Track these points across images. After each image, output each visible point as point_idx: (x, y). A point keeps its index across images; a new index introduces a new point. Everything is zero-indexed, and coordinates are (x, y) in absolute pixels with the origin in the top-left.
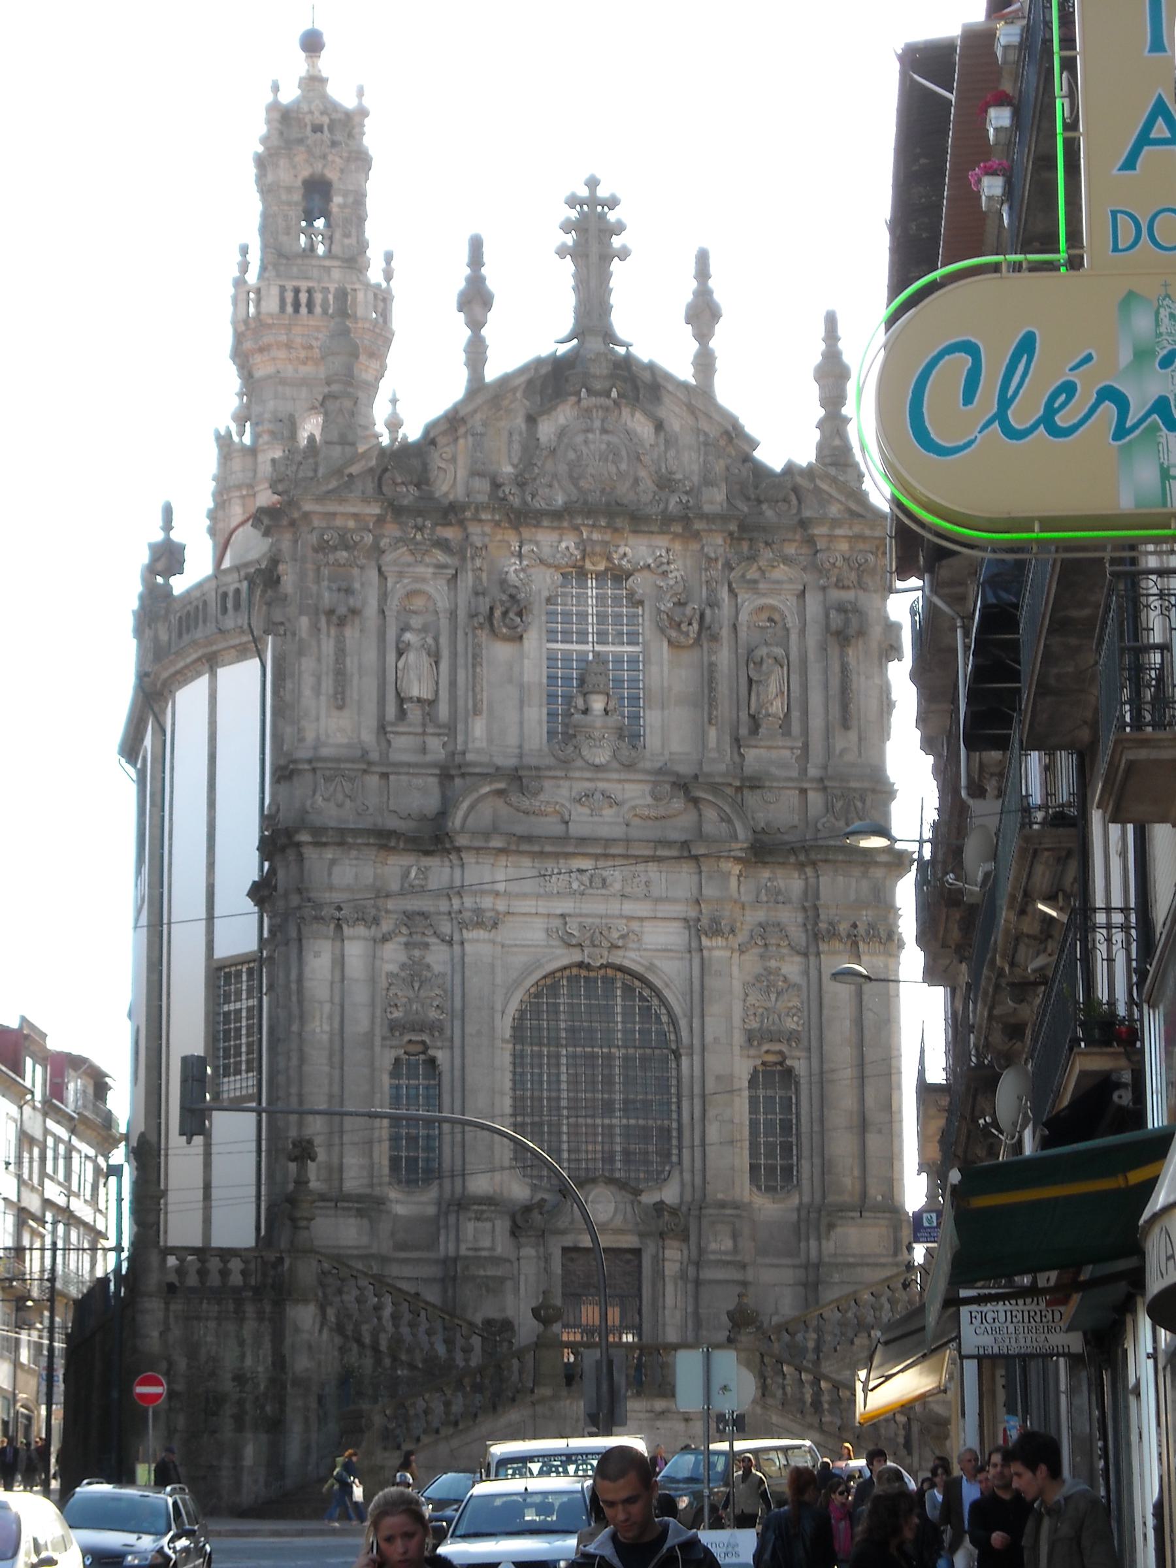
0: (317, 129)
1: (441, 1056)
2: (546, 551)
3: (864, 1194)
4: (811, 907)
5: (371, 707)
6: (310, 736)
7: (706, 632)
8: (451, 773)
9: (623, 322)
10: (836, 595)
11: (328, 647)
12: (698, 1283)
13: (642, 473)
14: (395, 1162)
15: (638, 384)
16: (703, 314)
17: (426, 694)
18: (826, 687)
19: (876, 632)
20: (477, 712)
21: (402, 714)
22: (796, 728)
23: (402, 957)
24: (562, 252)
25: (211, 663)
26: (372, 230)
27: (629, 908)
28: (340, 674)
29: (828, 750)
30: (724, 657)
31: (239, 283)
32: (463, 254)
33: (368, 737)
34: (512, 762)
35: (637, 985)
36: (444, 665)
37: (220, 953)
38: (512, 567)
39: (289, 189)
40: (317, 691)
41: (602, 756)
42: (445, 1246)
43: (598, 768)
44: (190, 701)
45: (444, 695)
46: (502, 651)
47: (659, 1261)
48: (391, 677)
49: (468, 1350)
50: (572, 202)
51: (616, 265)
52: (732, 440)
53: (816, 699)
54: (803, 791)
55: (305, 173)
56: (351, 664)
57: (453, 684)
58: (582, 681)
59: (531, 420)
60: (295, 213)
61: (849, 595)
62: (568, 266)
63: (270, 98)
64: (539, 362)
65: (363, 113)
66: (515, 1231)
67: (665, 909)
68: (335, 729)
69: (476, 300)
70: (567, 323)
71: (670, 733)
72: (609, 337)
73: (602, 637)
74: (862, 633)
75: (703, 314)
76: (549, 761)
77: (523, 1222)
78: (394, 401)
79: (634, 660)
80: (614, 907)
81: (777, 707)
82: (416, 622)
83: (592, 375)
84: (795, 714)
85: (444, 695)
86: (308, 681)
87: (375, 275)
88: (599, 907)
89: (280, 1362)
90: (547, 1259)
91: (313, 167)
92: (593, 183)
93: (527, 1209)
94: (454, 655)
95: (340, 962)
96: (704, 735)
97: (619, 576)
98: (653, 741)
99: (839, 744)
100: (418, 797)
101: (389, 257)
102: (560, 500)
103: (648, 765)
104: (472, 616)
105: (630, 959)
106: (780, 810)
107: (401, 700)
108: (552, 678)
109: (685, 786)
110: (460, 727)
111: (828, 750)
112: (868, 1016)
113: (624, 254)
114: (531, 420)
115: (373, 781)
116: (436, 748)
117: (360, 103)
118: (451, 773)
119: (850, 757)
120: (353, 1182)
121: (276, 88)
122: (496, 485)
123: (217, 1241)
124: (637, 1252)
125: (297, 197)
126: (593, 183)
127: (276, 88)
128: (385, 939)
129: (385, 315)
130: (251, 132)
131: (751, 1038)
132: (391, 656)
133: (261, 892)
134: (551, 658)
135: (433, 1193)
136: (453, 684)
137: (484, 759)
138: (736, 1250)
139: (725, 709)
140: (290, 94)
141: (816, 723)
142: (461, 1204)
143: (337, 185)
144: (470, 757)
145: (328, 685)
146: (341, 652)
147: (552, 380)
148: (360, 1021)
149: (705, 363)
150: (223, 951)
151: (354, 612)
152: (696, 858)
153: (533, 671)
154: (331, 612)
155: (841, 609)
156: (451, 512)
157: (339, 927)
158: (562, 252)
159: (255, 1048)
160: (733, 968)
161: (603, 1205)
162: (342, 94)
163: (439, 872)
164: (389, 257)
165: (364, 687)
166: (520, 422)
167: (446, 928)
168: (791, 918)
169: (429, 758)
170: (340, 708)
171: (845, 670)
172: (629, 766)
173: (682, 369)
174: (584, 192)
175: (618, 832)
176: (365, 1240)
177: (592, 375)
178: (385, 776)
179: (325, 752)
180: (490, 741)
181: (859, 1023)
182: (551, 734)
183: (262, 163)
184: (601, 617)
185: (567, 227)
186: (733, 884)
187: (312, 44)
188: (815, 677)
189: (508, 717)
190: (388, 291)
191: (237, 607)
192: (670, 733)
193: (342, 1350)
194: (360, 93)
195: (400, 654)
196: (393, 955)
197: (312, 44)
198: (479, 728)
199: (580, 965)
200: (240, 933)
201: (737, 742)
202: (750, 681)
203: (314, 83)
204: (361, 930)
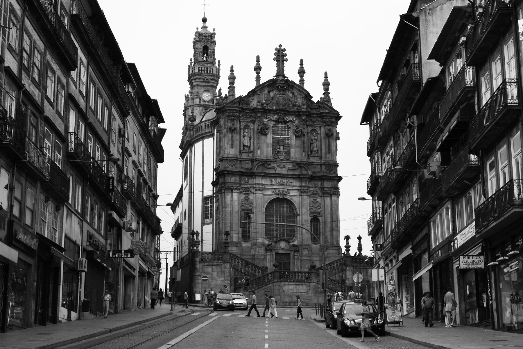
0: (206, 36)
1: (252, 215)
2: (272, 118)
3: (333, 243)
4: (322, 188)
5: (238, 147)
6: (226, 152)
9: (286, 74)
10: (327, 127)
11: (230, 135)
12: (301, 260)
13: (290, 103)
14: (242, 236)
16: (302, 72)
17: (249, 145)
18: (325, 145)
19: (335, 134)
20: (259, 149)
21: (244, 149)
22: (319, 153)
23: (244, 196)
25: (203, 138)
26: (216, 56)
28: (232, 140)
29: (326, 157)
31: (189, 66)
33: (238, 153)
34: (265, 158)
35: (289, 203)
36: (252, 139)
37: (205, 195)
38: (265, 121)
39: (200, 49)
40: (227, 144)
41: (282, 157)
42: (253, 252)
43: (282, 160)
44: (198, 146)
45: (252, 145)
46: (263, 137)
48: (242, 141)
49: (259, 272)
50: (276, 49)
52: (308, 96)
53: (323, 147)
54: (321, 165)
56: (234, 139)
57: (254, 143)
58: (278, 143)
59: (269, 92)
60: (201, 53)
61: (329, 128)
62: (276, 62)
63: (196, 30)
64: (270, 80)
65: (215, 34)
66: (266, 250)
67: (294, 188)
68: (230, 152)
69: (258, 69)
70: (275, 73)
71: (295, 153)
72: (284, 76)
73: (282, 134)
74: (332, 134)
75: (302, 72)
76: (272, 158)
77: (268, 249)
79: (288, 139)
81: (316, 149)
83: (280, 83)
84: (319, 150)
85: (252, 145)
86: (226, 142)
88: (282, 187)
90: (272, 255)
91: (205, 44)
92: (280, 46)
93: (268, 245)
94: (254, 137)
95: (232, 196)
96: (302, 155)
97: (285, 122)
98: (292, 155)
99: (328, 156)
101: (219, 62)
102: (274, 108)
103: (291, 159)
104: (258, 130)
105: (288, 197)
107: (244, 146)
108: (273, 142)
110: (255, 151)
111: (326, 157)
112: (334, 209)
113: (287, 60)
114: (269, 92)
115: (239, 162)
119: (330, 159)
120: (235, 240)
121: (197, 29)
122: (262, 104)
123: (204, 251)
124: (289, 254)
125: (201, 50)
126: (280, 46)
127: (197, 29)
128: (241, 192)
129: (219, 73)
130: (192, 37)
131: (311, 213)
132: (242, 137)
133: (214, 184)
134: (273, 138)
135: (250, 243)
136: (254, 143)
137: (260, 158)
138: (308, 254)
139: (306, 149)
140: (200, 30)
142: (256, 244)
143: (209, 48)
144: (257, 157)
145: (230, 143)
146: (232, 136)
148: (236, 208)
149: (302, 81)
150: (206, 194)
151: (235, 129)
152: (301, 178)
154: (230, 129)
155: (329, 130)
157: (232, 190)
159: (212, 213)
161: (283, 244)
162: (210, 30)
164: (219, 62)
165: (236, 143)
167: (253, 191)
169: (249, 158)
170: (232, 147)
172: (288, 160)
175: (286, 172)
176: (237, 251)
177: (280, 83)
178: (241, 161)
179: (229, 156)
180: (261, 154)
181: (331, 210)
182: (273, 153)
183: (194, 43)
184: (282, 130)
187: (204, 20)
188: (323, 143)
189: (265, 149)
191: (208, 127)
192: (295, 153)
193: (235, 272)
194: (214, 30)
195: (244, 136)
196: (243, 196)
197: (204, 20)
198: (259, 152)
199: (278, 198)
200: (209, 191)
201: (308, 155)
202: (311, 143)
203: (205, 27)
204: (236, 191)
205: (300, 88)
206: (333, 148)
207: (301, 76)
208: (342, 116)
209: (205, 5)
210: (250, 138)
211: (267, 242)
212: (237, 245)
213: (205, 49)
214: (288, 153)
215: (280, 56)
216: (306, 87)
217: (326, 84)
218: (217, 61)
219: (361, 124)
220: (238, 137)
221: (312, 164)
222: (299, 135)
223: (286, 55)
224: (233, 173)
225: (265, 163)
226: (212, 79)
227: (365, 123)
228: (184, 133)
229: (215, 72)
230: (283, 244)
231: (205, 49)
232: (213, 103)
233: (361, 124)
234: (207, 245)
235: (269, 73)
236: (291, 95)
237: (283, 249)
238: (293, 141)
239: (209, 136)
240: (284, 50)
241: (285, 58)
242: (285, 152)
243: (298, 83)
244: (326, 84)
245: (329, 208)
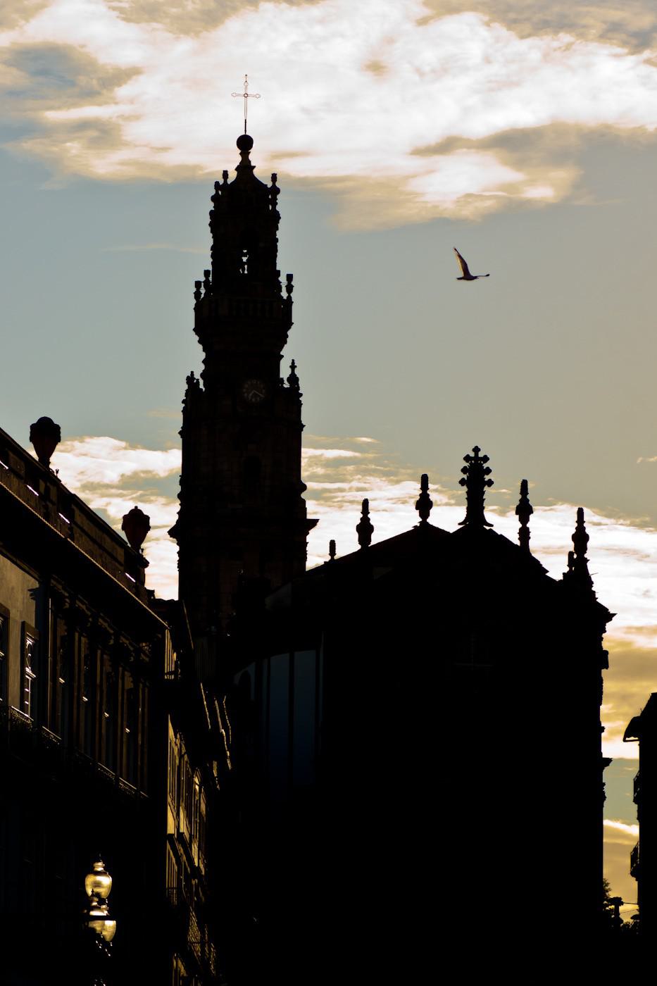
24: (462, 482)
44: (279, 663)
50: (467, 458)
51: (486, 488)
62: (465, 489)
78: (293, 367)
87: (284, 294)
92: (476, 450)
101: (290, 277)
113: (490, 483)
117: (274, 185)
121: (225, 174)
126: (476, 450)
127: (225, 174)
149: (524, 534)
158: (462, 482)
164: (290, 277)
173: (515, 539)
174: (472, 454)
185: (464, 470)
187: (245, 143)
190: (289, 298)
194: (274, 177)
197: (245, 143)
203: (245, 168)
208: (615, 614)
209: (246, 95)
218: (283, 279)
219: (625, 740)
223: (488, 471)
227: (632, 738)
233: (625, 740)
240: (486, 459)
241: (487, 478)
243: (518, 543)
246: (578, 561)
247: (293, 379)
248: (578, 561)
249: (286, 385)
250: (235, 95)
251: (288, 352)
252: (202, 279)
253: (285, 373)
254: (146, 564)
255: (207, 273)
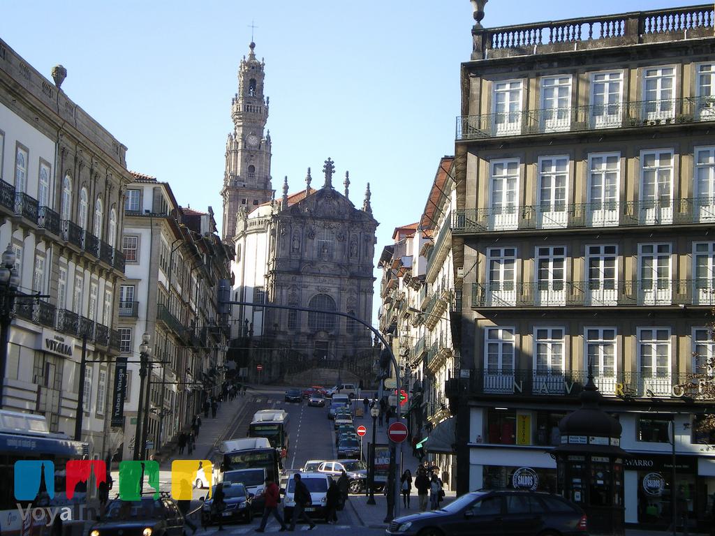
0: (253, 68)
4: (359, 287)
7: (344, 239)
8: (301, 261)
15: (336, 195)
16: (347, 183)
24: (324, 171)
27: (329, 285)
30: (347, 243)
32: (307, 171)
33: (288, 255)
35: (330, 298)
47: (331, 344)
50: (326, 162)
52: (351, 205)
55: (250, 78)
59: (317, 201)
67: (335, 286)
69: (309, 179)
71: (337, 256)
74: (370, 240)
75: (347, 183)
78: (268, 132)
80: (327, 285)
82: (296, 235)
83: (328, 193)
89: (271, 359)
92: (329, 159)
100: (295, 265)
101: (268, 98)
105: (328, 294)
106: (355, 269)
109: (340, 265)
113: (334, 172)
114: (317, 201)
116: (299, 257)
118: (301, 261)
126: (329, 159)
141: (361, 255)
143: (257, 82)
147: (321, 194)
149: (347, 192)
153: (315, 244)
156: (302, 217)
158: (324, 171)
160: (345, 296)
161: (322, 334)
162: (259, 59)
163: (298, 278)
164: (268, 98)
166: (315, 201)
168: (355, 288)
171: (367, 247)
173: (345, 195)
175: (328, 272)
177: (328, 193)
185: (324, 166)
186: (346, 282)
187: (252, 46)
188: (362, 247)
189: (311, 253)
192: (337, 256)
196: (290, 291)
197: (252, 46)
198: (306, 254)
201: (348, 257)
203: (252, 56)
205: (346, 198)
206: (371, 252)
207: (347, 187)
209: (253, 27)
210: (300, 242)
211: (309, 331)
212: (284, 333)
213: (253, 82)
214: (331, 256)
215: (329, 168)
216: (351, 198)
217: (369, 194)
218: (265, 99)
220: (289, 241)
221: (351, 265)
222: (342, 238)
223: (334, 167)
224: (283, 272)
225: (312, 263)
226: (260, 120)
228: (226, 180)
229: (263, 111)
230: (322, 334)
231: (253, 82)
232: (259, 148)
234: (258, 332)
235: (318, 184)
236: (336, 203)
237: (322, 338)
238: (337, 245)
239: (263, 232)
242: (329, 256)
244: (369, 194)
245: (364, 304)
246: (367, 202)
247: (268, 137)
248: (367, 202)
249: (266, 139)
250: (249, 26)
251: (267, 127)
252: (235, 97)
253: (265, 134)
254: (126, 149)
255: (236, 95)
